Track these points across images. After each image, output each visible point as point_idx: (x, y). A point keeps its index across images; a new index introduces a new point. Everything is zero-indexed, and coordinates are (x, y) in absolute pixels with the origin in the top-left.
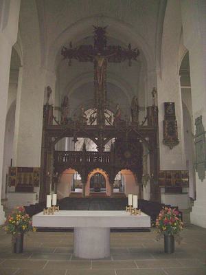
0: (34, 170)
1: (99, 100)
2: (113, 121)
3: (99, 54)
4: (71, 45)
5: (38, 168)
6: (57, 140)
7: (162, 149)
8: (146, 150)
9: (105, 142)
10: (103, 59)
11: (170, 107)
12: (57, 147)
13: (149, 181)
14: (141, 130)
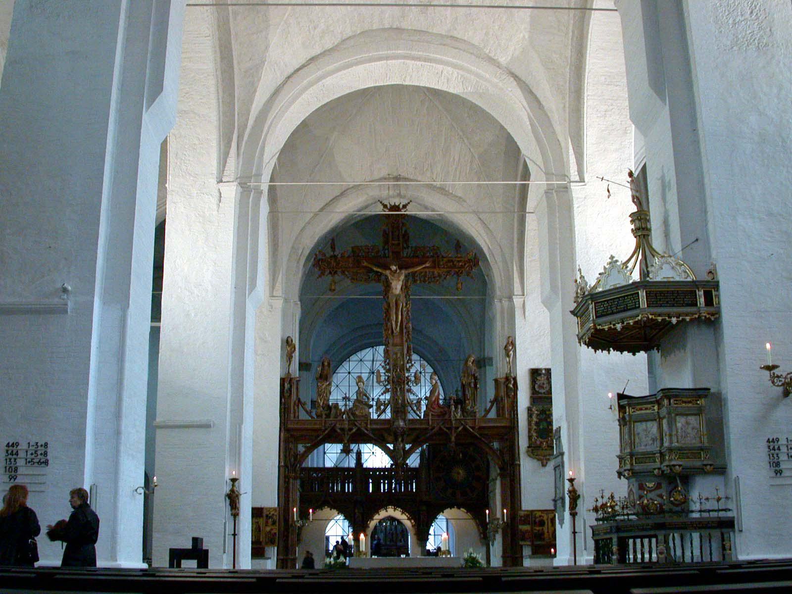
0: (265, 513)
1: (395, 366)
2: (424, 408)
3: (394, 268)
4: (333, 248)
5: (275, 509)
6: (309, 450)
7: (527, 466)
8: (495, 471)
9: (408, 454)
10: (402, 277)
11: (542, 379)
12: (312, 461)
13: (500, 531)
14: (481, 428)
